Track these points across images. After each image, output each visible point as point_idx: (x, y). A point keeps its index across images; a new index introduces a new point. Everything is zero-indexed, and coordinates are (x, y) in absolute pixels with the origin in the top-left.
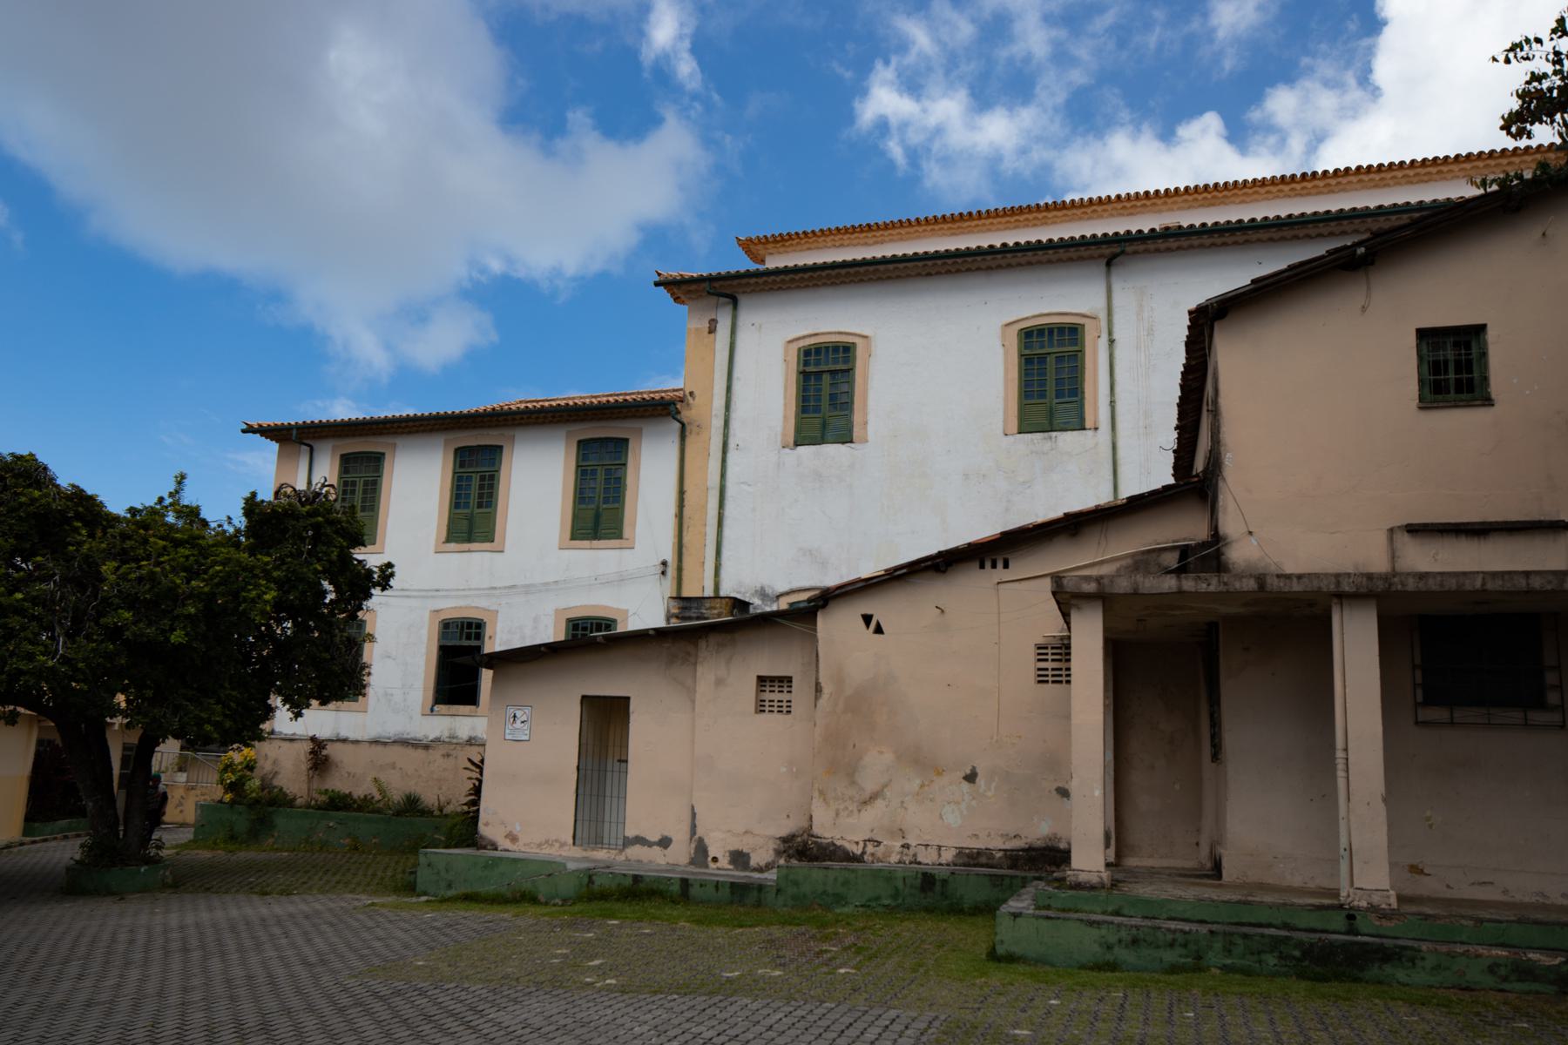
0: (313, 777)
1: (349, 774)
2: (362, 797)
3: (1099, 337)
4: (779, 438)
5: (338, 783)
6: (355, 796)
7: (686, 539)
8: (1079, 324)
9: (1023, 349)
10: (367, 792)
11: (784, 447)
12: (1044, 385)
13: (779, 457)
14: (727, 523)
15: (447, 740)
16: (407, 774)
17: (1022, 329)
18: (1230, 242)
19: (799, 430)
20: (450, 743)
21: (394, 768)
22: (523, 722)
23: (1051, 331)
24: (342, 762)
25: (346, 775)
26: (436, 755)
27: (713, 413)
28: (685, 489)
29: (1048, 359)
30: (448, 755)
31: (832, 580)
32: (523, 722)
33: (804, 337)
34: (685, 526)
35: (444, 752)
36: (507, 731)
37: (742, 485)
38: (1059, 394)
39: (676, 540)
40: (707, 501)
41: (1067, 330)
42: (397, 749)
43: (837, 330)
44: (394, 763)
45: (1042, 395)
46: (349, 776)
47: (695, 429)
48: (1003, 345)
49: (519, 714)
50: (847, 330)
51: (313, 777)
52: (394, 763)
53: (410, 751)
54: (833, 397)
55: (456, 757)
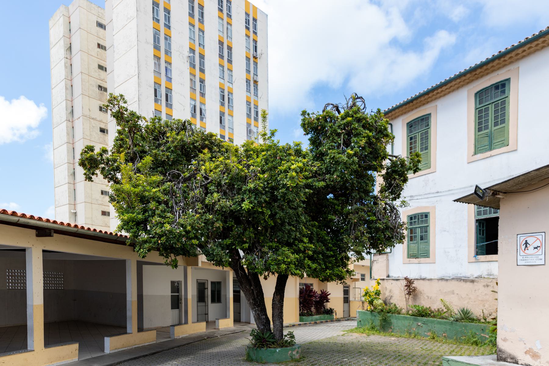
0: (409, 299)
1: (428, 297)
2: (436, 310)
5: (424, 303)
6: (433, 309)
10: (439, 307)
15: (486, 277)
16: (461, 297)
20: (488, 278)
21: (453, 294)
22: (535, 248)
24: (423, 290)
25: (427, 298)
26: (479, 286)
30: (488, 286)
32: (535, 248)
35: (485, 284)
36: (519, 258)
42: (455, 283)
44: (453, 291)
46: (428, 298)
49: (530, 240)
51: (409, 299)
52: (453, 291)
53: (462, 284)
55: (493, 287)
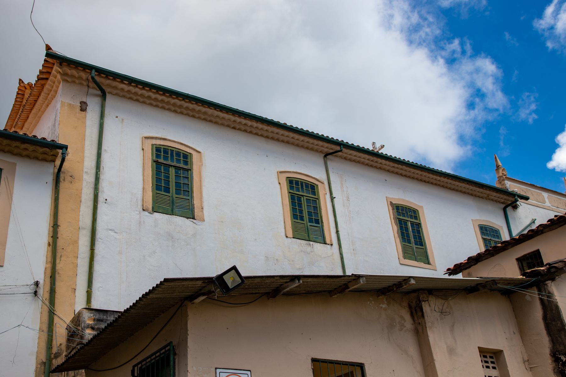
4: (140, 203)
7: (59, 267)
8: (315, 184)
11: (144, 210)
13: (140, 217)
14: (97, 258)
19: (155, 201)
27: (85, 170)
28: (59, 224)
33: (156, 138)
34: (58, 255)
37: (110, 231)
39: (49, 265)
40: (78, 238)
43: (179, 141)
47: (68, 178)
50: (186, 144)
54: (178, 184)
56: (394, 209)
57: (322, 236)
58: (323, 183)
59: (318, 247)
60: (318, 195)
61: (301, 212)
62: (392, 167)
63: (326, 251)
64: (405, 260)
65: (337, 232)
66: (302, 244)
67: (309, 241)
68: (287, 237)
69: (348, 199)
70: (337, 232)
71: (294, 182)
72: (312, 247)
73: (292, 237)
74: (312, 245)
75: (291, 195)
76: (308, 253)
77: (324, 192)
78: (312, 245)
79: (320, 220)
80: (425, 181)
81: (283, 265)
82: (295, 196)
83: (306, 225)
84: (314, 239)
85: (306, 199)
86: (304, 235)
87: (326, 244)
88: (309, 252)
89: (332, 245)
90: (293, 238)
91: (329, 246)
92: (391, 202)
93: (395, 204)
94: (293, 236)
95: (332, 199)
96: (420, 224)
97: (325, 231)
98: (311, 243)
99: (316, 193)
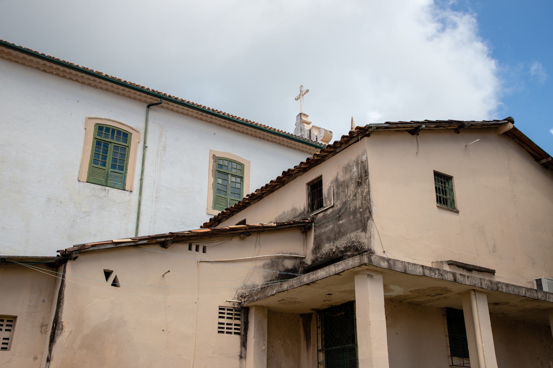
3: (139, 142)
9: (96, 135)
12: (106, 159)
17: (97, 124)
18: (204, 119)
23: (113, 131)
29: (110, 145)
31: (89, 240)
38: (113, 166)
41: (122, 133)
45: (104, 164)
48: (85, 129)
56: (215, 162)
57: (123, 182)
58: (138, 132)
59: (114, 193)
60: (130, 144)
61: (105, 158)
62: (223, 122)
63: (123, 197)
64: (214, 210)
65: (141, 179)
66: (96, 189)
67: (106, 186)
68: (79, 181)
69: (164, 149)
70: (141, 179)
71: (105, 128)
72: (107, 192)
73: (86, 181)
74: (108, 190)
75: (97, 141)
76: (100, 198)
77: (137, 141)
78: (108, 190)
79: (125, 168)
80: (260, 138)
81: (67, 207)
82: (102, 142)
83: (106, 171)
84: (112, 184)
85: (114, 146)
86: (101, 180)
87: (125, 190)
88: (101, 197)
89: (131, 191)
90: (87, 182)
91: (127, 193)
92: (214, 155)
93: (218, 157)
94: (87, 180)
95: (145, 147)
96: (242, 177)
97: (127, 177)
98: (107, 188)
99: (128, 141)
